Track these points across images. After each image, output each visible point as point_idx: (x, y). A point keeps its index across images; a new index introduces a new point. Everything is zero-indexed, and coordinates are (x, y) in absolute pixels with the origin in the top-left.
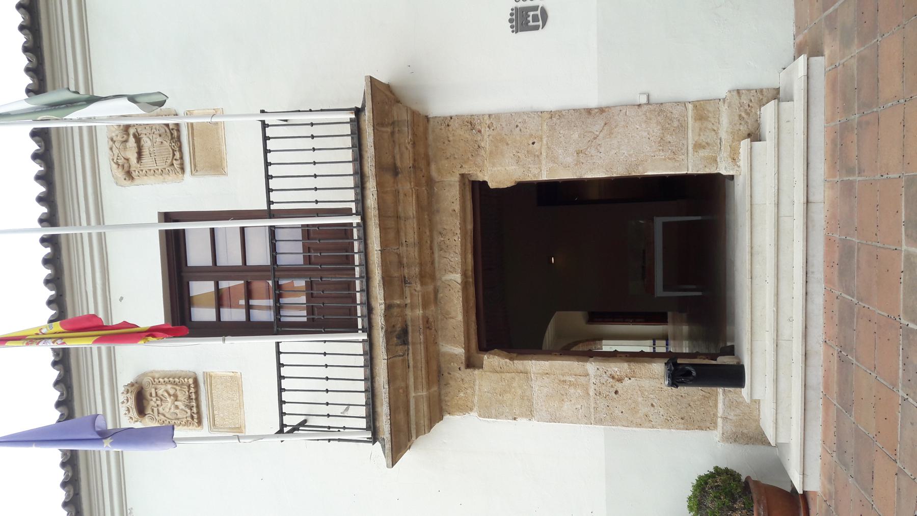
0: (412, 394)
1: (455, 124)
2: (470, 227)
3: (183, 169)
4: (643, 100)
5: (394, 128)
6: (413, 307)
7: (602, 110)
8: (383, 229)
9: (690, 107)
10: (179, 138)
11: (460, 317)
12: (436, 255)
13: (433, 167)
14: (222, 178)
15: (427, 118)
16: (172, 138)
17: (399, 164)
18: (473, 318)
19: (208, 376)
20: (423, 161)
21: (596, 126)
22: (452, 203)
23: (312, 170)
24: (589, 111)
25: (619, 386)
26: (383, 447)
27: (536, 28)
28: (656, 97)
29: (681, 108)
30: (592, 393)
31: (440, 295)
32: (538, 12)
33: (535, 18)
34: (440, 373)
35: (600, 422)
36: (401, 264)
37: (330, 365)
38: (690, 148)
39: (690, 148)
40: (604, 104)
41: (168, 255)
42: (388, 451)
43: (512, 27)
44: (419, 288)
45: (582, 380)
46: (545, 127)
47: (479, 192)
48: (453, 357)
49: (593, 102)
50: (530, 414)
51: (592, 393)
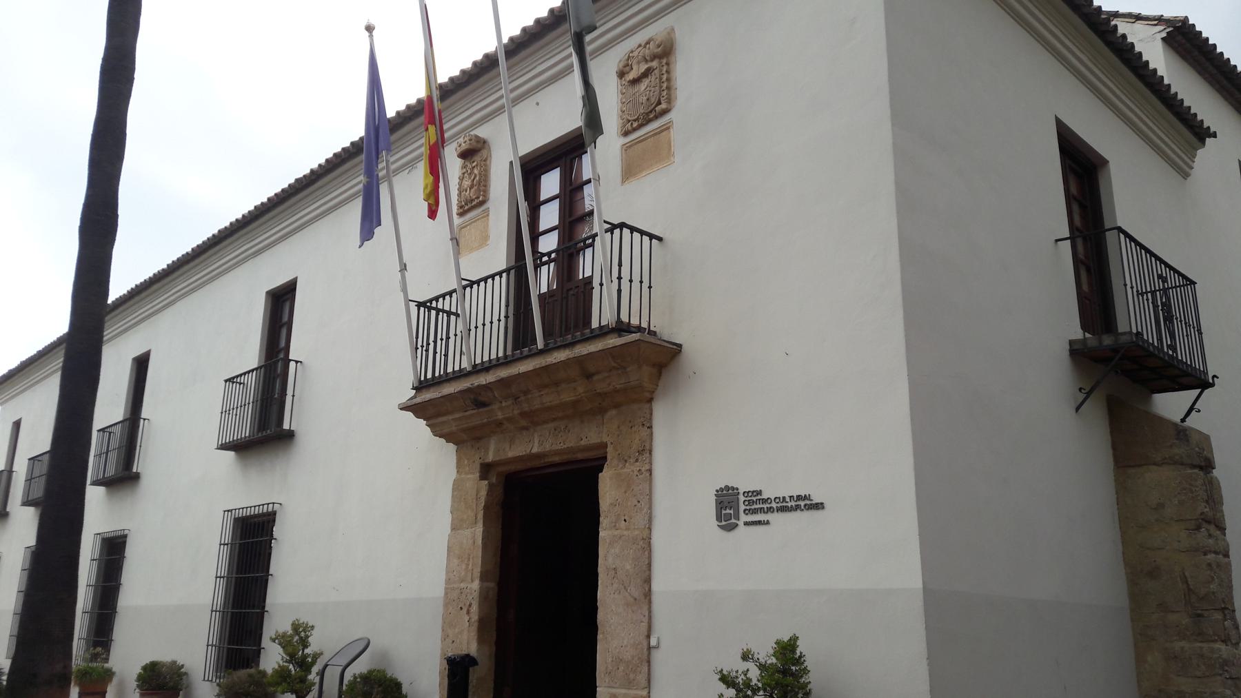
0: (451, 417)
1: (644, 432)
2: (580, 456)
3: (626, 134)
4: (653, 642)
5: (647, 365)
6: (501, 408)
7: (648, 594)
8: (536, 372)
9: (644, 693)
10: (649, 121)
11: (511, 454)
12: (551, 425)
13: (613, 412)
14: (619, 179)
15: (650, 400)
16: (647, 114)
17: (595, 378)
18: (520, 467)
19: (486, 214)
20: (595, 407)
21: (635, 591)
22: (587, 435)
23: (636, 278)
24: (648, 580)
25: (465, 610)
26: (415, 397)
27: (719, 518)
28: (657, 656)
29: (644, 683)
30: (462, 585)
31: (524, 433)
32: (733, 521)
33: (729, 517)
34: (478, 439)
35: (446, 594)
36: (526, 393)
37: (484, 333)
38: (614, 691)
39: (614, 691)
40: (656, 599)
41: (557, 147)
42: (410, 403)
43: (722, 489)
44: (516, 412)
45: (469, 579)
46: (637, 532)
47: (598, 464)
48: (487, 450)
49: (656, 586)
50: (454, 528)
51: (462, 585)
